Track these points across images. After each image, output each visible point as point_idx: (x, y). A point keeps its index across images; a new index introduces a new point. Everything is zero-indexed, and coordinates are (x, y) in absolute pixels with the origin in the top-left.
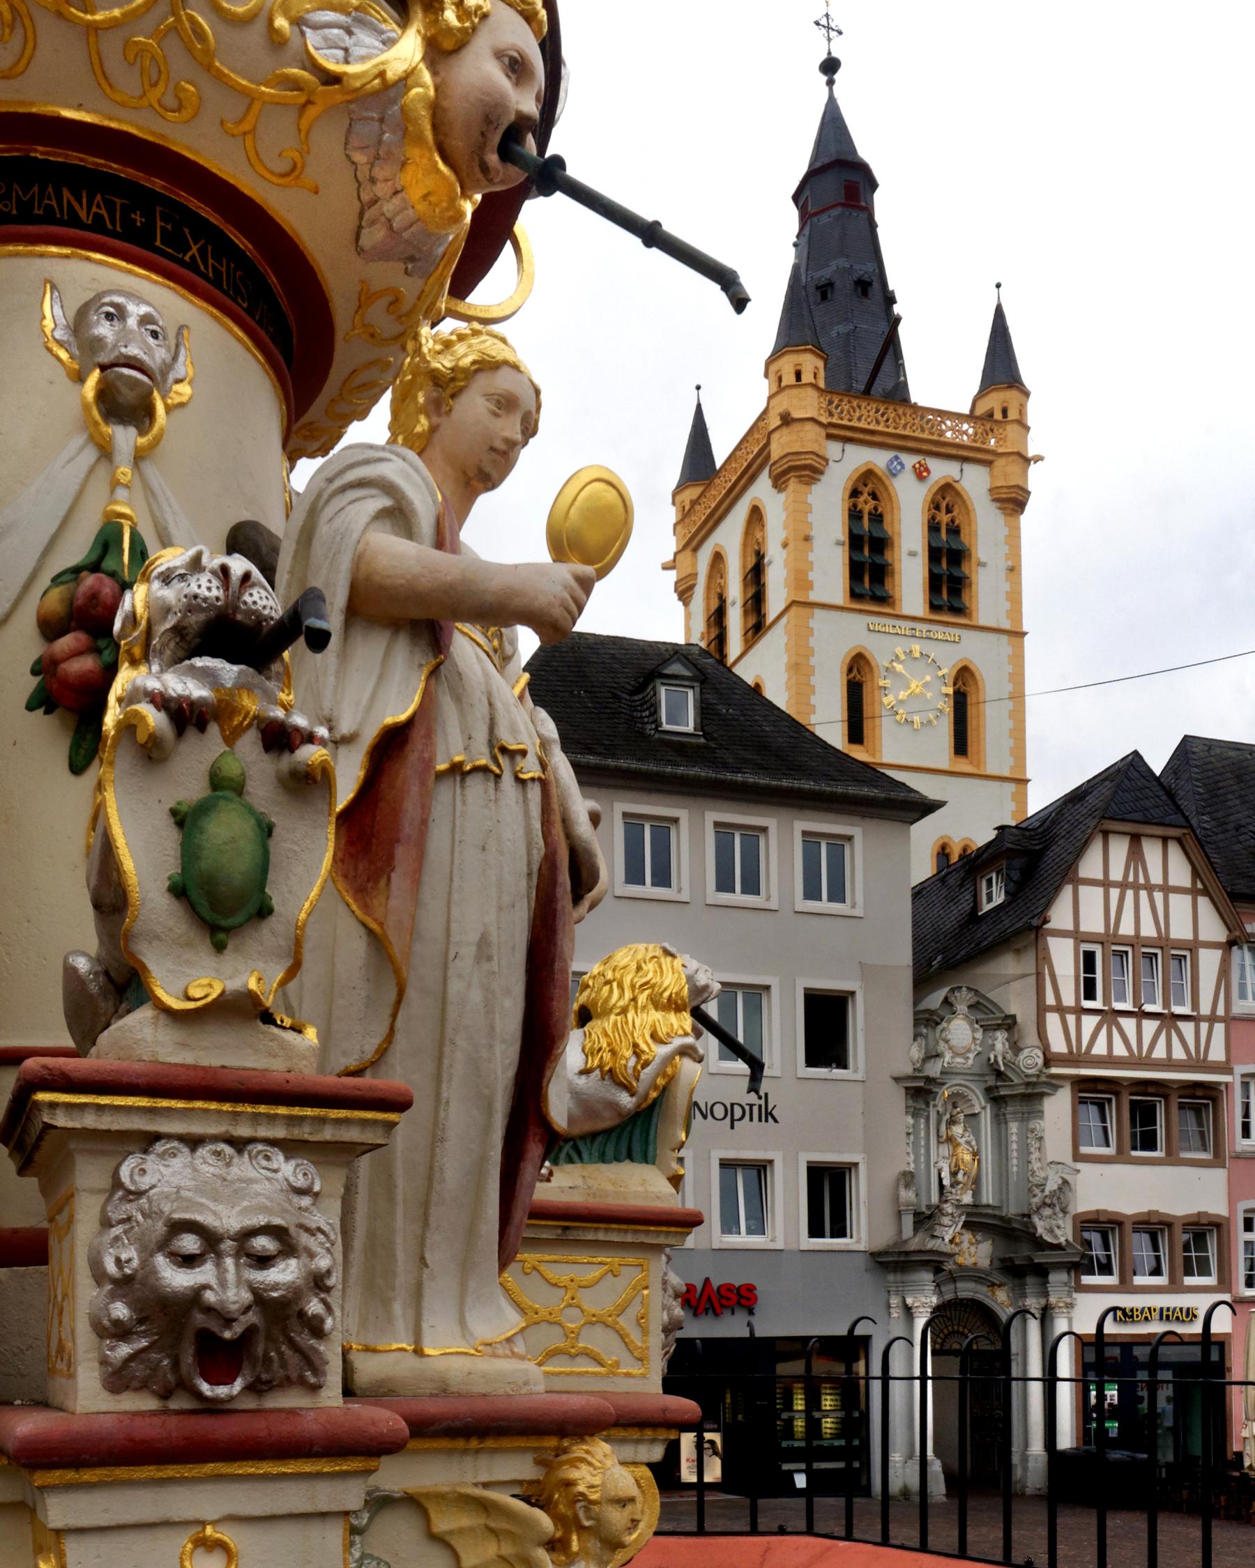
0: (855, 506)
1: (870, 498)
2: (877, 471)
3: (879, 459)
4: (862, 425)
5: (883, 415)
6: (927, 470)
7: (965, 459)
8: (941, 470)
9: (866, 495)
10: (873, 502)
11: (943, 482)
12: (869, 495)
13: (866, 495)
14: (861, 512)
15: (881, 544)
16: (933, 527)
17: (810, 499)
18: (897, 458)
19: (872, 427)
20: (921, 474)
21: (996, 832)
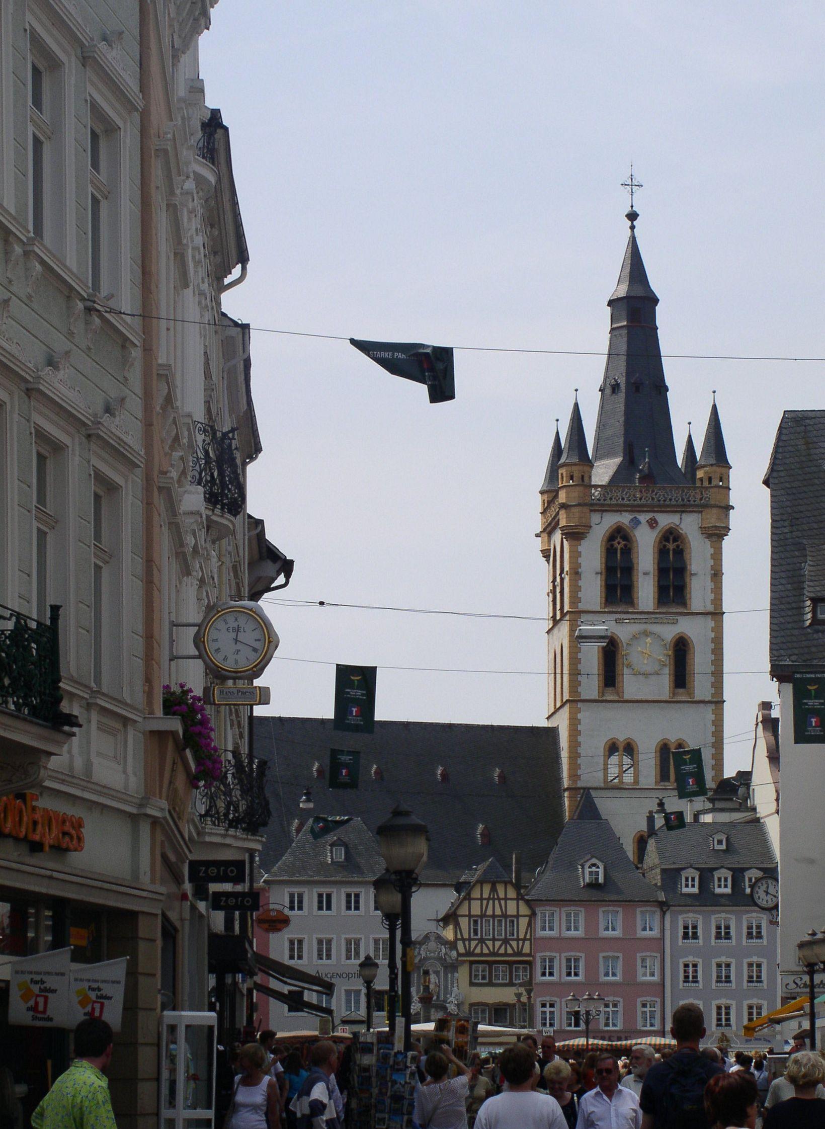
0: (612, 546)
1: (621, 541)
2: (624, 526)
3: (625, 519)
4: (614, 502)
5: (626, 494)
6: (656, 522)
7: (684, 512)
8: (665, 520)
9: (619, 539)
10: (624, 543)
11: (668, 527)
12: (621, 538)
13: (619, 539)
14: (616, 549)
15: (628, 570)
16: (662, 552)
17: (580, 549)
18: (635, 517)
19: (620, 501)
20: (653, 524)
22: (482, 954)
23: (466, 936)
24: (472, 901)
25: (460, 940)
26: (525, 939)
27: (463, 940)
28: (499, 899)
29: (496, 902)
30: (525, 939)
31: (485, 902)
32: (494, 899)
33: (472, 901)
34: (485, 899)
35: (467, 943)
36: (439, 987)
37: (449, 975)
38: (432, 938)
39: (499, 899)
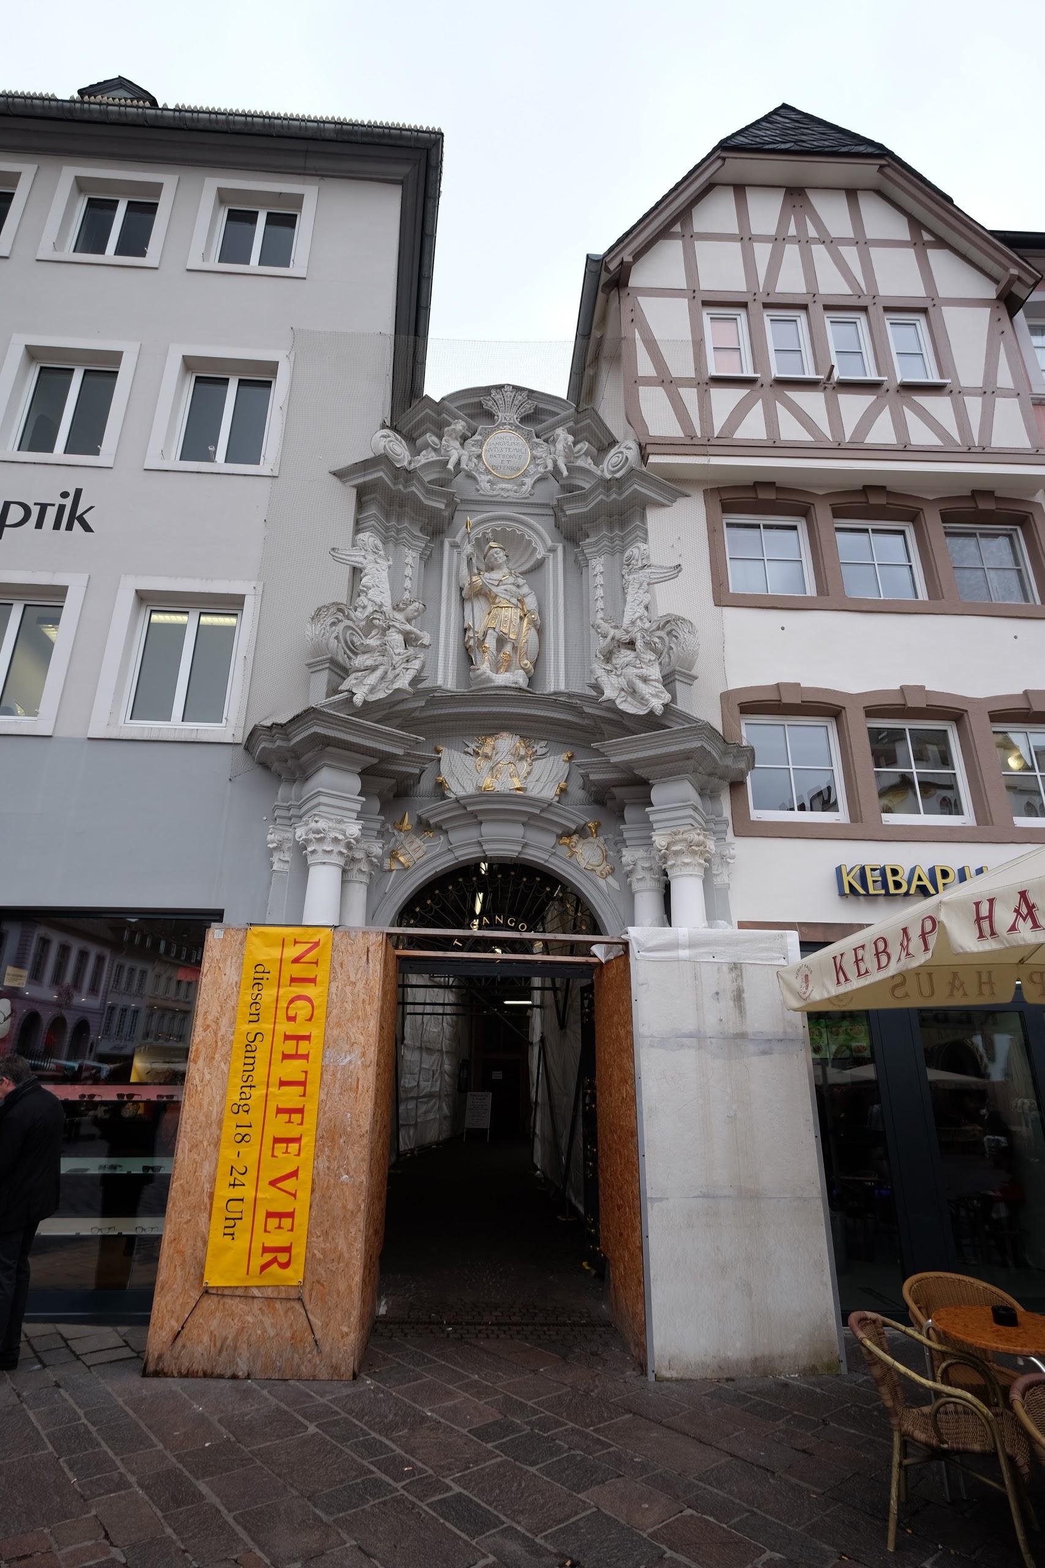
21: (623, 336)
22: (774, 446)
23: (681, 365)
24: (700, 246)
25: (648, 381)
26: (989, 392)
27: (666, 381)
28: (831, 243)
29: (819, 251)
30: (989, 392)
31: (762, 252)
32: (804, 242)
33: (700, 246)
34: (763, 239)
35: (690, 396)
36: (540, 631)
37: (598, 565)
38: (507, 415)
39: (831, 243)
